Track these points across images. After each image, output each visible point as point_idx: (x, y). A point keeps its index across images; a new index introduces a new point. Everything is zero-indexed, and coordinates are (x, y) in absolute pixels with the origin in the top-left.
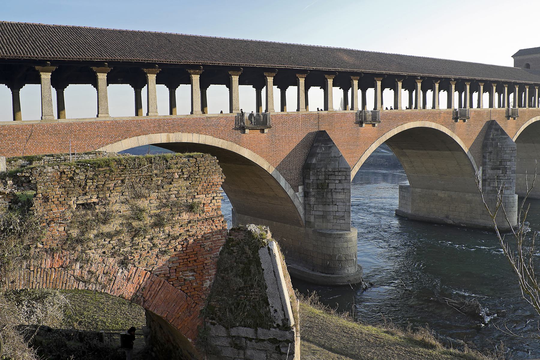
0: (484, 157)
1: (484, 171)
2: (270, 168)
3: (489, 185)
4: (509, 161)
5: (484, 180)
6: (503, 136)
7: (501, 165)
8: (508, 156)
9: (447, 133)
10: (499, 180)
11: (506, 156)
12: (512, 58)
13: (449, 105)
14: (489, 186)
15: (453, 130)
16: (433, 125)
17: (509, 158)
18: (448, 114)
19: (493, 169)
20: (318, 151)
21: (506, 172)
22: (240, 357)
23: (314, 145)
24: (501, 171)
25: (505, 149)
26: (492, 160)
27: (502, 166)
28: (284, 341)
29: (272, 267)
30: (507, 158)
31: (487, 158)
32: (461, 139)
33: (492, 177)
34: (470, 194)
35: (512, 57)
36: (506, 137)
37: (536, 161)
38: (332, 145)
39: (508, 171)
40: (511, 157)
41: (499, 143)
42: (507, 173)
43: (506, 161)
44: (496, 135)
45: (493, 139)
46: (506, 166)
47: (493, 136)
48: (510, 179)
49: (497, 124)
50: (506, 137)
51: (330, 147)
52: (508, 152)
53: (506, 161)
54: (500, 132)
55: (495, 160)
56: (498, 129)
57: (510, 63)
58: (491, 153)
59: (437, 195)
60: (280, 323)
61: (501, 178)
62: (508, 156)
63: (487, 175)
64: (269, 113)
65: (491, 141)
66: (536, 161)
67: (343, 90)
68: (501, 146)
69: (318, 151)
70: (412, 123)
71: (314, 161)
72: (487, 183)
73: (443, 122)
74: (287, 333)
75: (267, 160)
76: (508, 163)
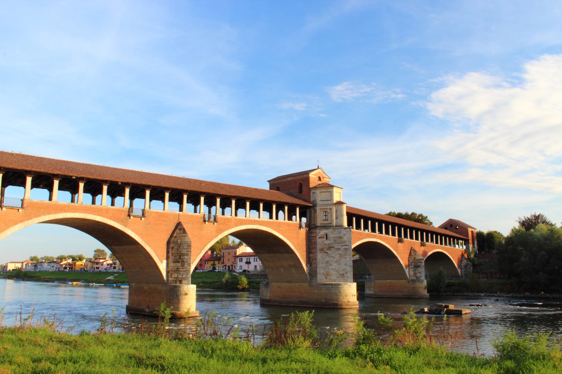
0: (168, 252)
1: (168, 264)
3: (171, 277)
4: (186, 255)
5: (168, 272)
7: (180, 259)
8: (185, 251)
10: (178, 272)
11: (184, 251)
12: (268, 183)
14: (171, 277)
17: (186, 253)
18: (118, 211)
19: (174, 262)
21: (184, 264)
24: (180, 264)
25: (184, 245)
26: (173, 255)
27: (181, 260)
30: (185, 253)
31: (170, 252)
32: (137, 234)
33: (173, 270)
34: (161, 285)
35: (268, 181)
37: (282, 269)
39: (185, 263)
40: (188, 252)
41: (179, 240)
42: (185, 265)
43: (184, 255)
44: (179, 234)
45: (175, 237)
46: (184, 260)
47: (177, 234)
48: (186, 271)
49: (182, 225)
50: (185, 235)
53: (184, 255)
54: (182, 231)
55: (176, 255)
56: (182, 229)
57: (267, 187)
58: (173, 248)
59: (143, 287)
61: (180, 270)
62: (185, 251)
63: (170, 268)
65: (174, 239)
66: (282, 269)
68: (181, 242)
72: (170, 274)
73: (111, 217)
76: (186, 257)
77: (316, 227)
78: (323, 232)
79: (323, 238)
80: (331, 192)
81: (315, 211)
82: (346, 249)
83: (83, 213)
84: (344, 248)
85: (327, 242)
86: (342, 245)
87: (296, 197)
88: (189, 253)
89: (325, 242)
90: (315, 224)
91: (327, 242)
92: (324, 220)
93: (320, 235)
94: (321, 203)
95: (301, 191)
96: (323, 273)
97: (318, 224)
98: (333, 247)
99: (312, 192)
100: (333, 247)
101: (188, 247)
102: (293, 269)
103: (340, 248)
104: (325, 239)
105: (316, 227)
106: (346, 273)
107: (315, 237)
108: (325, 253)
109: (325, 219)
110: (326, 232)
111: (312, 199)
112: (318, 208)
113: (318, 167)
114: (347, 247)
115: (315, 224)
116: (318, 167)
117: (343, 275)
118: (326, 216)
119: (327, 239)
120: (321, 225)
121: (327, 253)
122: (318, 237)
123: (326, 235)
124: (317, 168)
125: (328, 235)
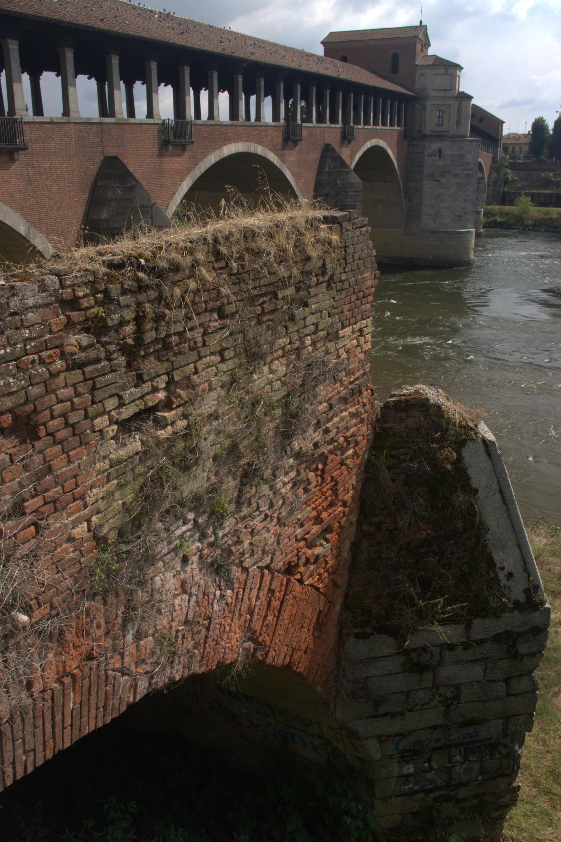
2: (31, 231)
6: (344, 170)
9: (275, 163)
13: (276, 117)
15: (282, 158)
16: (259, 150)
17: (353, 204)
20: (110, 195)
22: (422, 686)
23: (99, 184)
28: (526, 632)
29: (496, 482)
30: (350, 204)
32: (292, 173)
36: (347, 170)
38: (134, 183)
47: (330, 168)
51: (132, 188)
52: (351, 194)
60: (522, 598)
62: (351, 200)
64: (19, 117)
67: (95, 82)
69: (110, 195)
70: (233, 144)
71: (104, 215)
74: (537, 614)
75: (25, 216)
77: (424, 137)
78: (435, 146)
79: (435, 156)
80: (452, 75)
81: (424, 108)
82: (467, 175)
83: (246, 141)
84: (466, 174)
85: (441, 163)
86: (463, 170)
87: (385, 78)
88: (357, 203)
89: (438, 163)
90: (420, 131)
91: (441, 163)
92: (436, 125)
93: (430, 150)
94: (435, 93)
95: (395, 69)
96: (430, 214)
97: (428, 133)
98: (449, 172)
99: (418, 72)
100: (449, 172)
101: (356, 194)
102: (380, 207)
103: (459, 174)
104: (437, 158)
105: (424, 137)
106: (465, 214)
107: (422, 153)
108: (435, 181)
109: (437, 121)
110: (441, 146)
111: (418, 86)
112: (429, 104)
113: (421, 22)
114: (471, 172)
115: (420, 131)
116: (421, 22)
117: (461, 216)
118: (439, 117)
119: (440, 157)
120: (433, 133)
121: (439, 181)
122: (426, 153)
123: (440, 151)
124: (418, 24)
125: (442, 150)
